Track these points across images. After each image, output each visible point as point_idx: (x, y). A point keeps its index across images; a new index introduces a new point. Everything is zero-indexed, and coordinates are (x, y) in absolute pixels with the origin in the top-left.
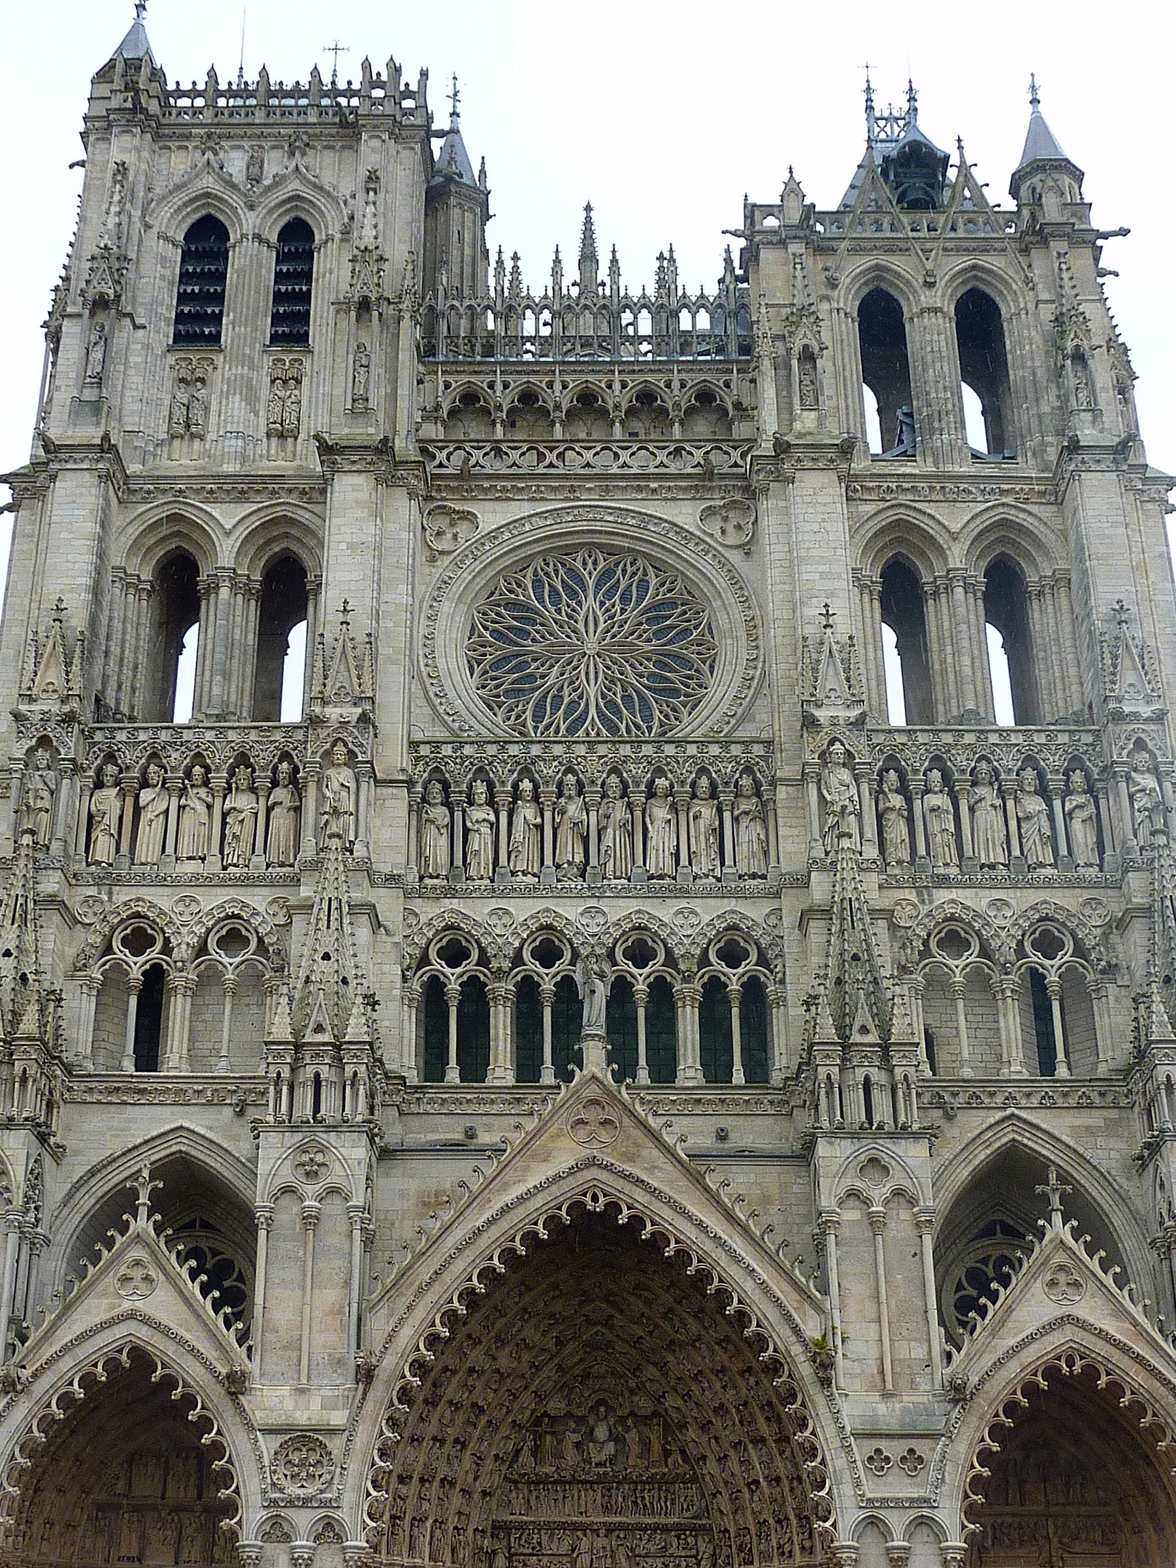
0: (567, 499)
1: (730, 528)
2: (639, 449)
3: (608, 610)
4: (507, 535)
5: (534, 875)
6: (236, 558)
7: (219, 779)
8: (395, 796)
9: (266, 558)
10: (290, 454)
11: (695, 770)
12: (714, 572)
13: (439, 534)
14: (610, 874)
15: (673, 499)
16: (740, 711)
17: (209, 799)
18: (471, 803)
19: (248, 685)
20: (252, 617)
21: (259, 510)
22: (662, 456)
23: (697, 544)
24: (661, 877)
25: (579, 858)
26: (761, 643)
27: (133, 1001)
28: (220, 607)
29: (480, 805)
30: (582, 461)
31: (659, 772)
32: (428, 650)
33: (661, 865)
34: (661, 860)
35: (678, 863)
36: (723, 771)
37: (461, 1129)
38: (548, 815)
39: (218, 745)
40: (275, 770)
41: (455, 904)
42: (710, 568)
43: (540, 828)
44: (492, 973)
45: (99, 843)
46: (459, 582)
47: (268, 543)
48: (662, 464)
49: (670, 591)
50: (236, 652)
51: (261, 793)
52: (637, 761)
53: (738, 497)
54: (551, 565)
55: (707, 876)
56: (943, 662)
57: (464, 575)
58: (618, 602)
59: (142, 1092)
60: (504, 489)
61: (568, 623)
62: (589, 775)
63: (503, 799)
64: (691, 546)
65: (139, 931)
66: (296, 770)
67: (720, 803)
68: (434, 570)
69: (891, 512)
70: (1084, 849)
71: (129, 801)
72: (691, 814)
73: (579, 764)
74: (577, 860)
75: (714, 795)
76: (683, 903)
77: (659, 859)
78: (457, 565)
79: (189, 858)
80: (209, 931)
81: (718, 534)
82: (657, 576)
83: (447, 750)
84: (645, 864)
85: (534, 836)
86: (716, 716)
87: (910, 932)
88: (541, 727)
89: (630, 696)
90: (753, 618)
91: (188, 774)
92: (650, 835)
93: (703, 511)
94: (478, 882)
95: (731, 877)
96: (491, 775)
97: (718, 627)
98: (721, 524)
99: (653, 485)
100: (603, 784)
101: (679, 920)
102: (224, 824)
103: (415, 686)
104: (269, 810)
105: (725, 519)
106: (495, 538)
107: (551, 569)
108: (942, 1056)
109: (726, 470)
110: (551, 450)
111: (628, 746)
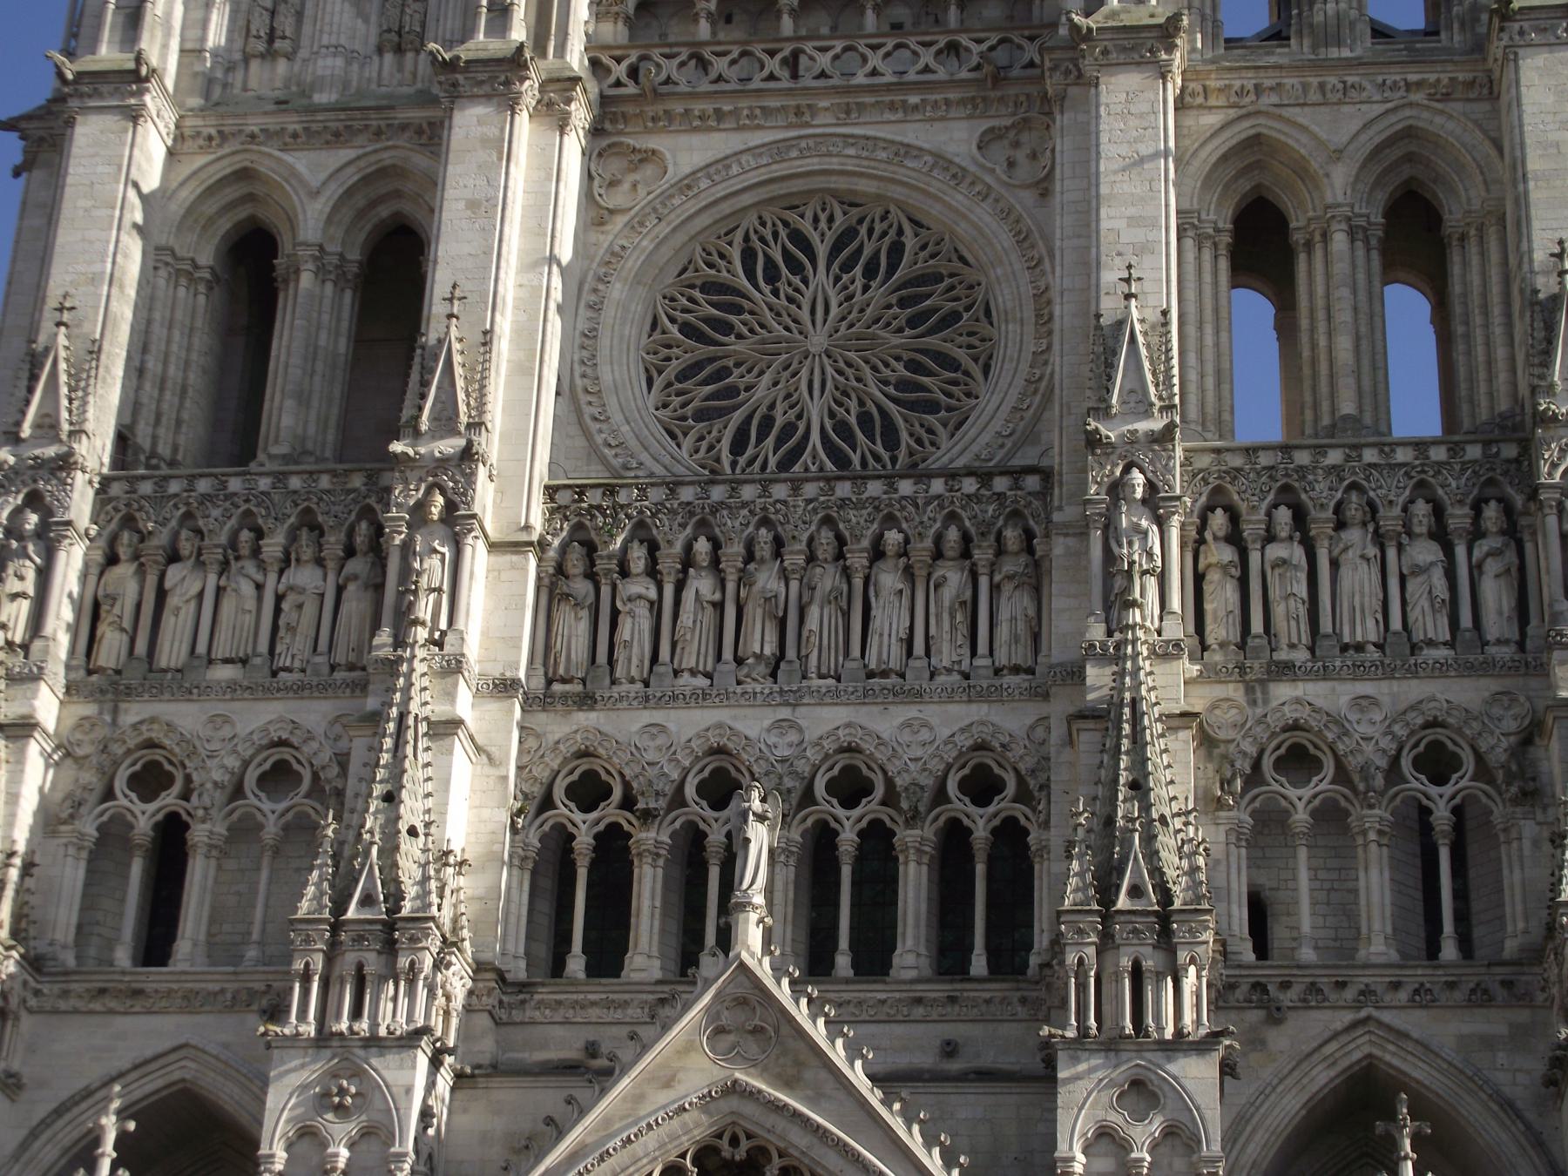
0: (789, 126)
1: (1021, 156)
2: (898, 46)
5: (708, 675)
6: (325, 230)
7: (273, 546)
9: (369, 227)
10: (408, 75)
11: (940, 517)
13: (613, 184)
17: (259, 577)
19: (335, 411)
20: (346, 314)
22: (927, 57)
24: (884, 674)
27: (137, 868)
28: (300, 300)
31: (890, 521)
33: (885, 656)
36: (980, 517)
37: (580, 1044)
38: (731, 587)
39: (276, 498)
40: (351, 533)
43: (719, 606)
45: (105, 643)
47: (373, 204)
48: (926, 69)
50: (320, 366)
51: (331, 565)
52: (859, 505)
54: (769, 224)
55: (949, 671)
56: (1314, 346)
57: (645, 243)
59: (138, 993)
63: (669, 563)
64: (963, 188)
65: (152, 768)
68: (602, 238)
69: (1246, 124)
70: (1497, 621)
71: (151, 580)
74: (768, 651)
75: (966, 554)
76: (911, 712)
77: (885, 648)
79: (226, 661)
80: (246, 764)
83: (594, 497)
87: (1232, 747)
91: (233, 543)
92: (873, 613)
95: (982, 672)
99: (914, 99)
100: (811, 540)
101: (906, 737)
102: (278, 611)
104: (340, 590)
105: (1016, 145)
106: (689, 187)
107: (767, 233)
108: (1279, 933)
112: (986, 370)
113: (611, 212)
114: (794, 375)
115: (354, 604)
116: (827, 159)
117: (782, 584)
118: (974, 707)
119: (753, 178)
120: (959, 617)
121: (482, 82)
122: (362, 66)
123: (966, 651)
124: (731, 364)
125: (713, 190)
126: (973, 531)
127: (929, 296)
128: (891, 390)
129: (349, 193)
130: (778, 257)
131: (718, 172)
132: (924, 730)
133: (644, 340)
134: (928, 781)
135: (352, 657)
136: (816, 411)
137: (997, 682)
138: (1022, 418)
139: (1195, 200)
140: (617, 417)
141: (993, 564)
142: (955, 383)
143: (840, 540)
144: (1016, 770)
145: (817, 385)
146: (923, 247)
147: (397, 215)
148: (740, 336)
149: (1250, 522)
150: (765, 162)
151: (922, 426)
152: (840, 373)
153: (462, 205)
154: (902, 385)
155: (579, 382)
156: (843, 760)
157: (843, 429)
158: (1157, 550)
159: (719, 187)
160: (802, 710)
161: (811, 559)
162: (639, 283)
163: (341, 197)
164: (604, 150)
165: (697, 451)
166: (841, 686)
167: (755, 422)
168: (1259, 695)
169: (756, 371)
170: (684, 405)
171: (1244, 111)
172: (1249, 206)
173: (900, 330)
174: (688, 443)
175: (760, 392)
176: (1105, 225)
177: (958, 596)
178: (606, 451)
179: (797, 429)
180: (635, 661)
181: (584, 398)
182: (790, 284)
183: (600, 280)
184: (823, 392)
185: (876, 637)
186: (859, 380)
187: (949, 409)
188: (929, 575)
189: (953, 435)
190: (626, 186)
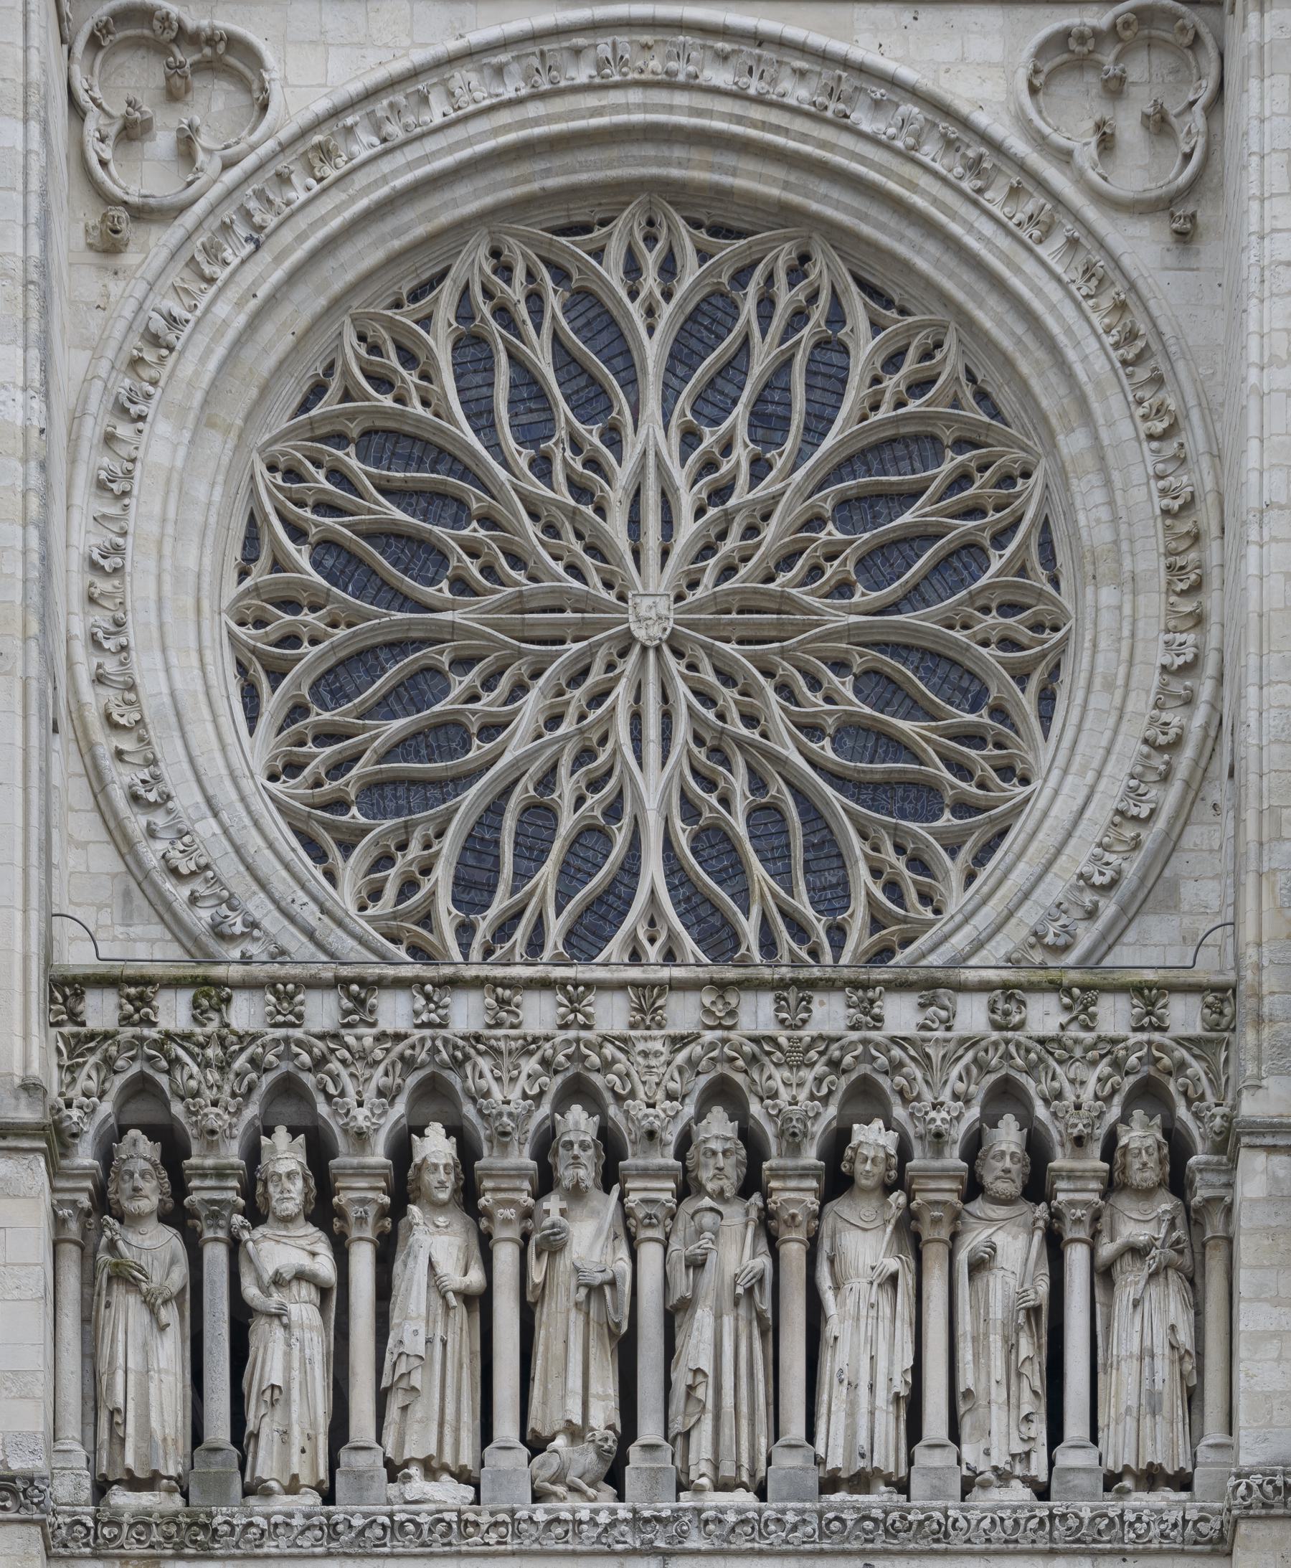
1: (1129, 127)
3: (709, 465)
4: (364, 144)
5: (463, 1476)
11: (979, 1090)
12: (1069, 311)
14: (700, 1469)
18: (257, 1214)
23: (1015, 192)
24: (861, 1482)
25: (604, 1413)
26: (1212, 601)
29: (287, 1220)
32: (101, 618)
33: (863, 1440)
34: (863, 1421)
35: (914, 1432)
38: (506, 1256)
46: (202, 340)
49: (919, 386)
54: (519, 274)
55: (1004, 1477)
58: (742, 433)
61: (573, 515)
62: (637, 1107)
64: (995, 198)
67: (1056, 1215)
68: (116, 288)
72: (963, 1257)
73: (607, 1065)
81: (1086, 151)
82: (876, 327)
84: (811, 1436)
86: (1055, 888)
88: (484, 925)
89: (774, 809)
90: (1188, 505)
92: (833, 1328)
93: (1042, 50)
94: (282, 1503)
95: (1082, 1481)
96: (323, 1109)
97: (1075, 535)
98: (1100, 110)
100: (686, 1141)
105: (1115, 88)
106: (325, 152)
107: (516, 293)
111: (766, 1002)
116: (661, 97)
117: (624, 1253)
123: (1039, 1429)
125: (385, 166)
141: (1096, 1218)
143: (750, 1137)
150: (509, 93)
155: (87, 692)
159: (399, 159)
161: (687, 1188)
162: (211, 424)
177: (1022, 1295)
178: (168, 885)
180: (297, 1439)
181: (106, 743)
185: (841, 1392)
188: (954, 1236)
190: (163, 142)
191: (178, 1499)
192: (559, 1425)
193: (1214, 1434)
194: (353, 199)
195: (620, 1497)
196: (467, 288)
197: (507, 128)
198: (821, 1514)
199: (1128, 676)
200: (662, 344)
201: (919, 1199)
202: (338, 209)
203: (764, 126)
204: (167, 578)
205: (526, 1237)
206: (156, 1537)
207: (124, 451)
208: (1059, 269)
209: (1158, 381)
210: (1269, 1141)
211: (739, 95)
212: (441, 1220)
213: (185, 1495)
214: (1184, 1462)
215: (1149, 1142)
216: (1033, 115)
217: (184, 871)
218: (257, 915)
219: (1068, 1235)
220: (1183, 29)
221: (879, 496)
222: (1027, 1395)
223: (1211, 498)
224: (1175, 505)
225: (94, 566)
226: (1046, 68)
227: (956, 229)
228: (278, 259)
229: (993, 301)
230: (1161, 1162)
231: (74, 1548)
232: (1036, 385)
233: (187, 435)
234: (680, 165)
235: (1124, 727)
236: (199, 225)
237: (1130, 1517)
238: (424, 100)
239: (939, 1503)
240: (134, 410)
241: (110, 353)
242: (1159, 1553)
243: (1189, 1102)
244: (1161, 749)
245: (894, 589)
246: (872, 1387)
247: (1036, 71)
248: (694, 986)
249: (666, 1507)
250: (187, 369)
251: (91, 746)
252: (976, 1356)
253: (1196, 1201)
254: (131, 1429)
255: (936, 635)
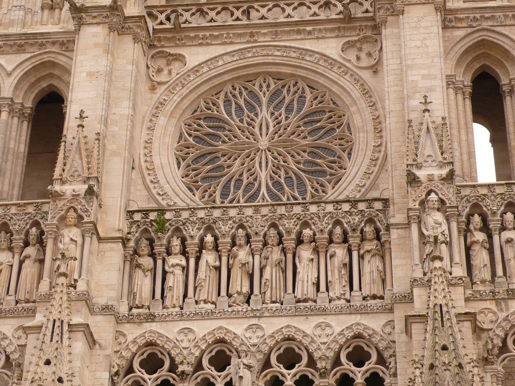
0: (248, 42)
1: (363, 55)
4: (205, 69)
5: (213, 303)
8: (112, 249)
9: (36, 92)
11: (331, 222)
12: (351, 87)
13: (159, 71)
14: (268, 300)
15: (323, 38)
16: (368, 183)
21: (31, 57)
24: (306, 301)
25: (246, 289)
26: (384, 134)
29: (176, 254)
30: (259, 15)
31: (306, 225)
32: (147, 151)
33: (305, 292)
35: (318, 290)
36: (352, 222)
38: (224, 259)
40: (27, 233)
41: (154, 326)
42: (348, 84)
43: (218, 269)
44: (178, 376)
46: (171, 103)
47: (38, 81)
48: (315, 14)
50: (10, 157)
51: (16, 250)
52: (290, 218)
53: (369, 33)
54: (238, 89)
55: (339, 298)
57: (175, 98)
60: (204, 38)
63: (192, 249)
64: (335, 69)
66: (42, 233)
68: (154, 96)
69: (476, 35)
75: (345, 240)
76: (321, 319)
78: (171, 91)
84: (294, 292)
85: (214, 274)
87: (491, 333)
92: (298, 270)
93: (344, 44)
94: (171, 310)
97: (354, 125)
99: (309, 28)
100: (265, 235)
101: (318, 332)
103: (135, 175)
104: (21, 263)
105: (360, 50)
106: (197, 71)
107: (237, 92)
109: (360, 15)
110: (238, 8)
112: (350, 154)
113: (160, 83)
114: (252, 160)
115: (29, 270)
116: (266, 58)
117: (251, 257)
118: (353, 316)
119: (230, 67)
120: (343, 272)
121: (95, 17)
122: (33, 16)
123: (348, 288)
124: (220, 155)
125: (210, 73)
126: (349, 229)
127: (319, 121)
128: (302, 166)
129: (26, 74)
130: (242, 103)
131: (212, 63)
132: (327, 328)
133: (176, 145)
134: (331, 354)
135: (28, 296)
136: (263, 175)
137: (365, 303)
138: (369, 178)
139: (453, 70)
140: (162, 181)
141: (359, 245)
142: (334, 162)
143: (280, 235)
144: (377, 349)
145: (264, 164)
146: (315, 98)
147: (50, 86)
148: (224, 142)
149: (492, 221)
150: (235, 59)
151: (318, 183)
152: (275, 158)
153: (84, 75)
154: (306, 162)
156: (285, 345)
157: (277, 184)
158: (447, 232)
159: (212, 71)
160: (262, 319)
161: (265, 244)
162: (172, 117)
163: (22, 76)
164: (155, 54)
165: (203, 197)
166: (283, 307)
167: (233, 183)
168: (503, 305)
169: (232, 158)
170: (196, 175)
171: (475, 29)
172: (475, 79)
173: (305, 138)
174: (198, 193)
175: (234, 169)
176: (411, 78)
179: (254, 185)
180: (175, 297)
182: (248, 117)
183: (154, 116)
184: (267, 166)
186: (285, 162)
187: (331, 175)
188: (327, 251)
189: (334, 187)
190: (166, 72)
191: (147, 310)
192: (235, 292)
193: (388, 287)
194: (203, 78)
195: (249, 306)
196: (227, 92)
197: (235, 65)
198: (295, 308)
199: (366, 148)
200: (267, 99)
201: (318, 243)
202: (200, 80)
203: (287, 61)
204: (161, 143)
205: (229, 255)
206: (142, 318)
207: (154, 122)
208: (349, 80)
209: (371, 97)
210: (397, 227)
211: (282, 56)
212: (210, 253)
213: (149, 309)
214: (381, 293)
215: (371, 230)
216: (342, 54)
217: (161, 194)
218: (176, 201)
219: (353, 249)
220: (373, 39)
221: (313, 122)
222: (344, 281)
223: (383, 115)
224: (375, 117)
225: (146, 142)
226: (345, 47)
227: (327, 75)
228: (187, 89)
229: (335, 86)
230: (374, 234)
231: (123, 321)
232: (345, 99)
233: (167, 119)
234: (270, 68)
235: (366, 157)
236: (171, 84)
237: (369, 305)
238: (218, 61)
239: (324, 304)
240: (156, 115)
241: (152, 106)
242: (377, 313)
243: (380, 222)
244: (374, 160)
245: (315, 138)
246: (307, 281)
247: (343, 48)
248: (267, 205)
249: (259, 307)
250: (168, 108)
251: (143, 173)
252: (332, 274)
253: (381, 241)
254: (138, 296)
255: (325, 144)
